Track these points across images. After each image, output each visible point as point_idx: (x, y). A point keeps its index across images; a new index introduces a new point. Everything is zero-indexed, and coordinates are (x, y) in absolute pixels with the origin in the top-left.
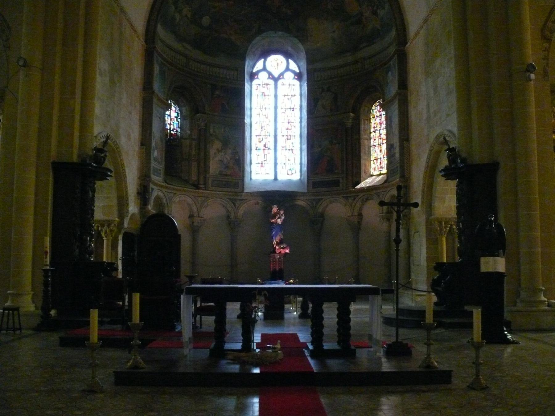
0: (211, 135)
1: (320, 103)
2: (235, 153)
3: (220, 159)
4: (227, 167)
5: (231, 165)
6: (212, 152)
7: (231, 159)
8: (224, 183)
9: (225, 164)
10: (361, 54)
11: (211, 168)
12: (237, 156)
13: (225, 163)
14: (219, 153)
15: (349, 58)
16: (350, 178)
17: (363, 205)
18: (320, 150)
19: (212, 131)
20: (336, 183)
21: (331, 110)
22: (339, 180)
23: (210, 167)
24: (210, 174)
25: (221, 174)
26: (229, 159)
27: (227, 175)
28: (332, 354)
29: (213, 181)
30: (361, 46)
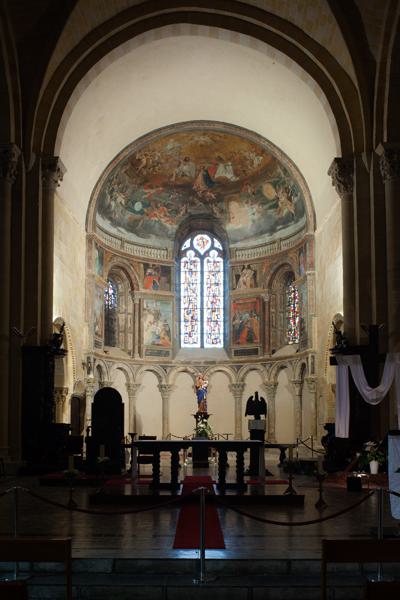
0: (144, 309)
1: (241, 279)
4: (159, 337)
5: (162, 335)
6: (145, 324)
10: (278, 235)
15: (267, 238)
16: (267, 346)
17: (278, 371)
20: (255, 352)
21: (251, 286)
25: (153, 344)
28: (231, 487)
29: (147, 350)
30: (278, 228)
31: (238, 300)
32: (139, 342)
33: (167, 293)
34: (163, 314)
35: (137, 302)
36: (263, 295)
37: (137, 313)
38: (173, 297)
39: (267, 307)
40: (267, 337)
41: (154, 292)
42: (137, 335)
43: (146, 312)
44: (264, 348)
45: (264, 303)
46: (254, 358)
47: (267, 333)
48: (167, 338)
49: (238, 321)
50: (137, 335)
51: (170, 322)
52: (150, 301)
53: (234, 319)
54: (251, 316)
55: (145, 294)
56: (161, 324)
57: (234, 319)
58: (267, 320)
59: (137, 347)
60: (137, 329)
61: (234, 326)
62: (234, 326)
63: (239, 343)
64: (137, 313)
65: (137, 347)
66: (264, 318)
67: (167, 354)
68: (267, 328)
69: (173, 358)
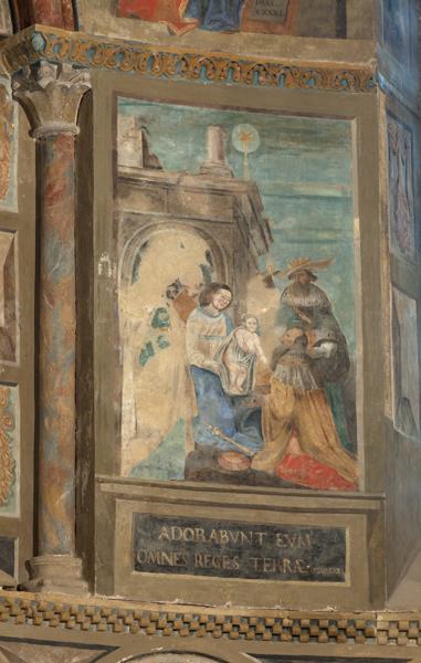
2: (309, 311)
3: (198, 359)
4: (251, 418)
5: (279, 402)
7: (277, 356)
8: (225, 536)
9: (234, 400)
11: (126, 431)
12: (320, 335)
13: (234, 391)
14: (184, 317)
19: (129, 155)
23: (118, 424)
24: (125, 471)
25: (205, 469)
26: (265, 360)
27: (246, 479)
32: (85, 452)
33: (315, 54)
34: (285, 223)
35: (62, 122)
37: (62, 214)
38: (363, 81)
41: (205, 41)
42: (62, 405)
43: (138, 205)
48: (318, 424)
50: (62, 405)
51: (342, 288)
52: (180, 114)
55: (125, 54)
56: (263, 304)
59: (60, 500)
60: (61, 353)
64: (62, 214)
65: (60, 500)
67: (323, 557)
69: (377, 596)
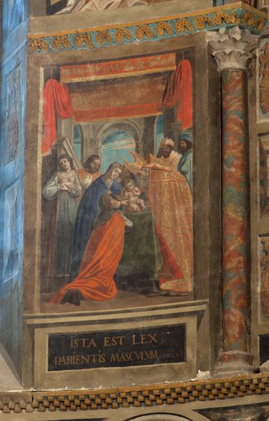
16: (234, 315)
18: (89, 180)
22: (182, 328)
31: (74, 63)
36: (211, 36)
39: (233, 106)
40: (234, 263)
44: (218, 323)
45: (219, 82)
46: (160, 377)
47: (234, 243)
49: (71, 180)
53: (53, 165)
54: (145, 148)
57: (53, 165)
58: (233, 170)
61: (49, 204)
62: (49, 204)
63: (73, 299)
66: (220, 160)
68: (233, 213)
